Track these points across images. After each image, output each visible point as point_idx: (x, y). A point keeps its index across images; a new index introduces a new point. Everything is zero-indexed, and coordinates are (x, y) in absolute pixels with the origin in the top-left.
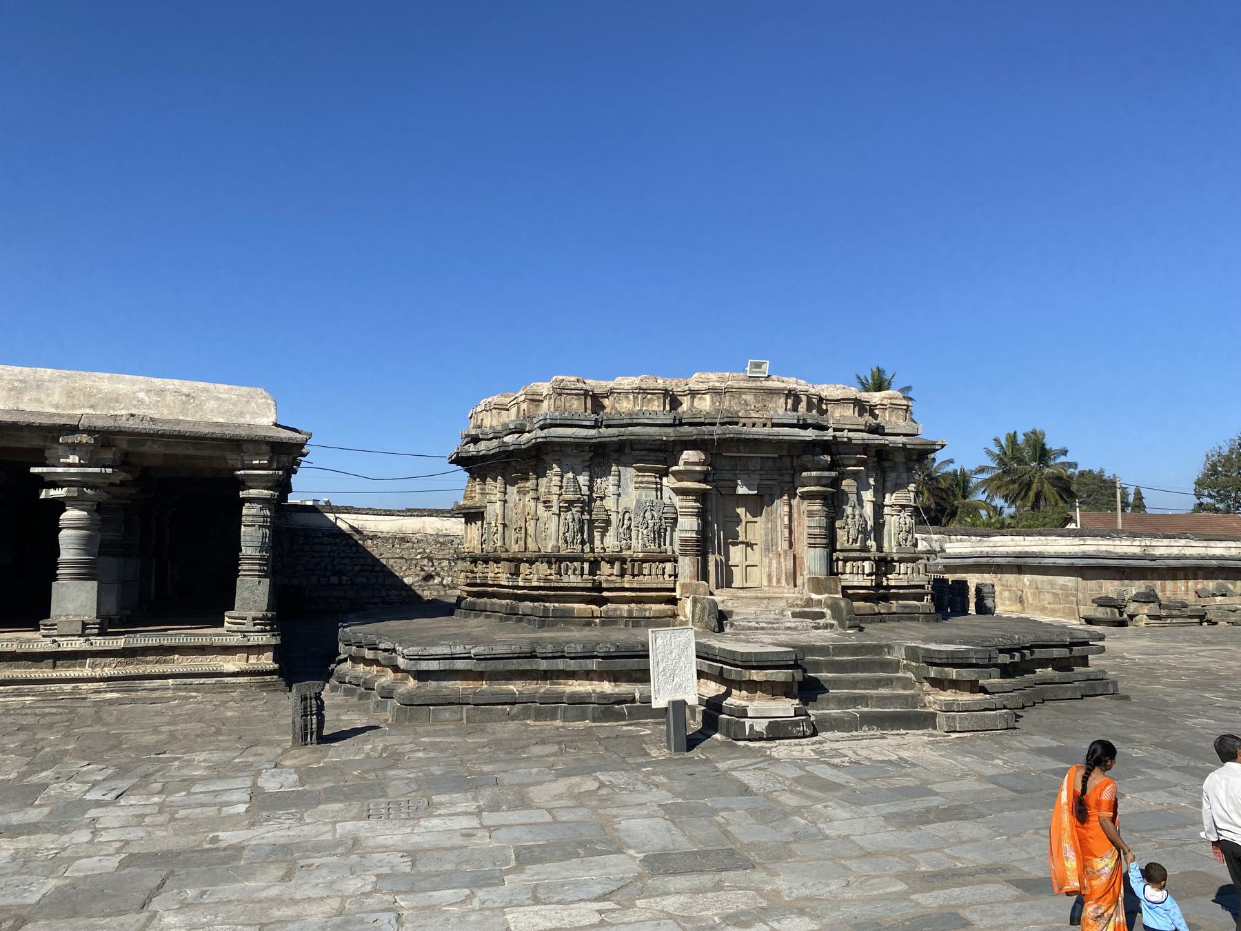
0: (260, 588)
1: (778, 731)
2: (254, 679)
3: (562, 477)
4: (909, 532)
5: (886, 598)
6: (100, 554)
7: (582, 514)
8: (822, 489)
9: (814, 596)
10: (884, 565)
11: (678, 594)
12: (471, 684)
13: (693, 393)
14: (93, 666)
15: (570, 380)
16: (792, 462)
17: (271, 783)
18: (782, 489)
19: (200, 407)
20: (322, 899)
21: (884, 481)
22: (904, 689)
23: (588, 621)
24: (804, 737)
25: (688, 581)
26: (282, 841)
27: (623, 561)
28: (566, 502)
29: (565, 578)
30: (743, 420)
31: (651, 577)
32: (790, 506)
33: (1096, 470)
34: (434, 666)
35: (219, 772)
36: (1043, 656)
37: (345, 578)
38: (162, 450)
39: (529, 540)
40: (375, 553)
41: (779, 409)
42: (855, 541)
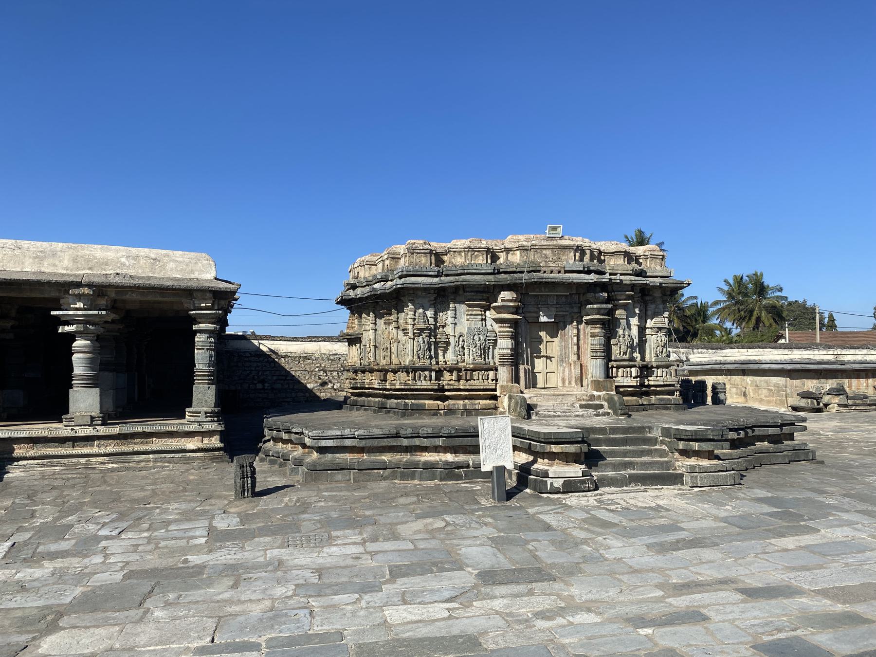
1: (570, 487)
3: (415, 312)
4: (664, 347)
5: (647, 394)
6: (100, 370)
8: (601, 317)
9: (596, 393)
10: (646, 370)
11: (498, 393)
12: (356, 456)
13: (507, 250)
14: (99, 446)
15: (419, 243)
16: (579, 298)
17: (221, 524)
19: (163, 267)
20: (259, 600)
21: (646, 310)
22: (661, 457)
23: (435, 412)
24: (589, 491)
25: (505, 383)
26: (231, 562)
27: (459, 370)
28: (418, 329)
29: (419, 383)
30: (544, 269)
31: (479, 381)
32: (578, 330)
33: (801, 301)
34: (330, 443)
35: (187, 516)
36: (761, 433)
37: (266, 385)
38: (139, 298)
39: (393, 356)
40: (287, 367)
41: (570, 260)
42: (625, 353)
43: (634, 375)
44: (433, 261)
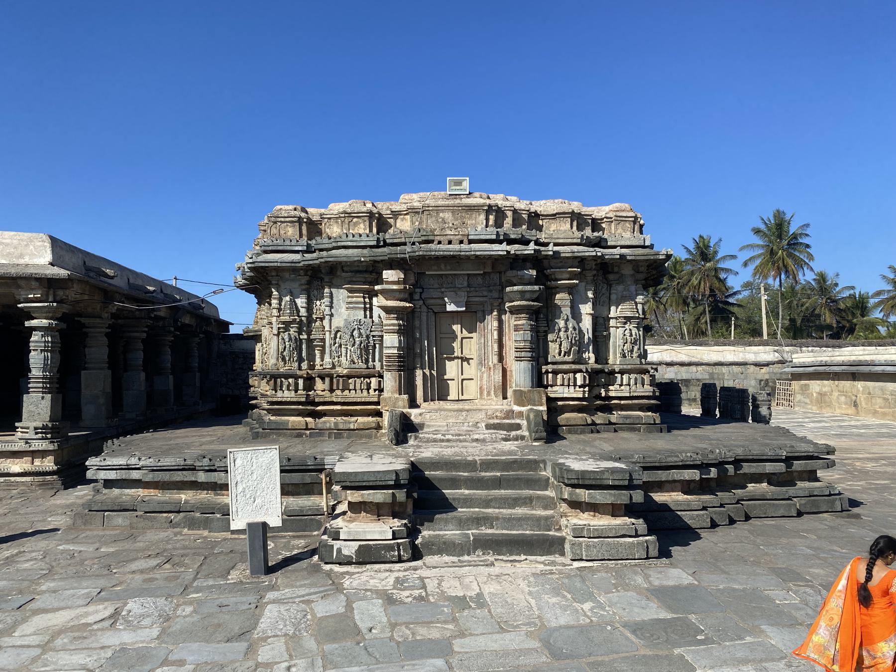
0: (43, 402)
1: (368, 555)
2: (37, 479)
4: (634, 343)
5: (608, 409)
7: (300, 333)
9: (516, 408)
12: (152, 492)
13: (396, 214)
18: (492, 304)
21: (610, 294)
22: (546, 508)
24: (400, 561)
25: (390, 395)
27: (331, 377)
28: (283, 323)
29: (279, 394)
30: (438, 238)
32: (501, 322)
34: (112, 475)
36: (753, 470)
42: (567, 353)
43: (579, 383)
44: (304, 232)
